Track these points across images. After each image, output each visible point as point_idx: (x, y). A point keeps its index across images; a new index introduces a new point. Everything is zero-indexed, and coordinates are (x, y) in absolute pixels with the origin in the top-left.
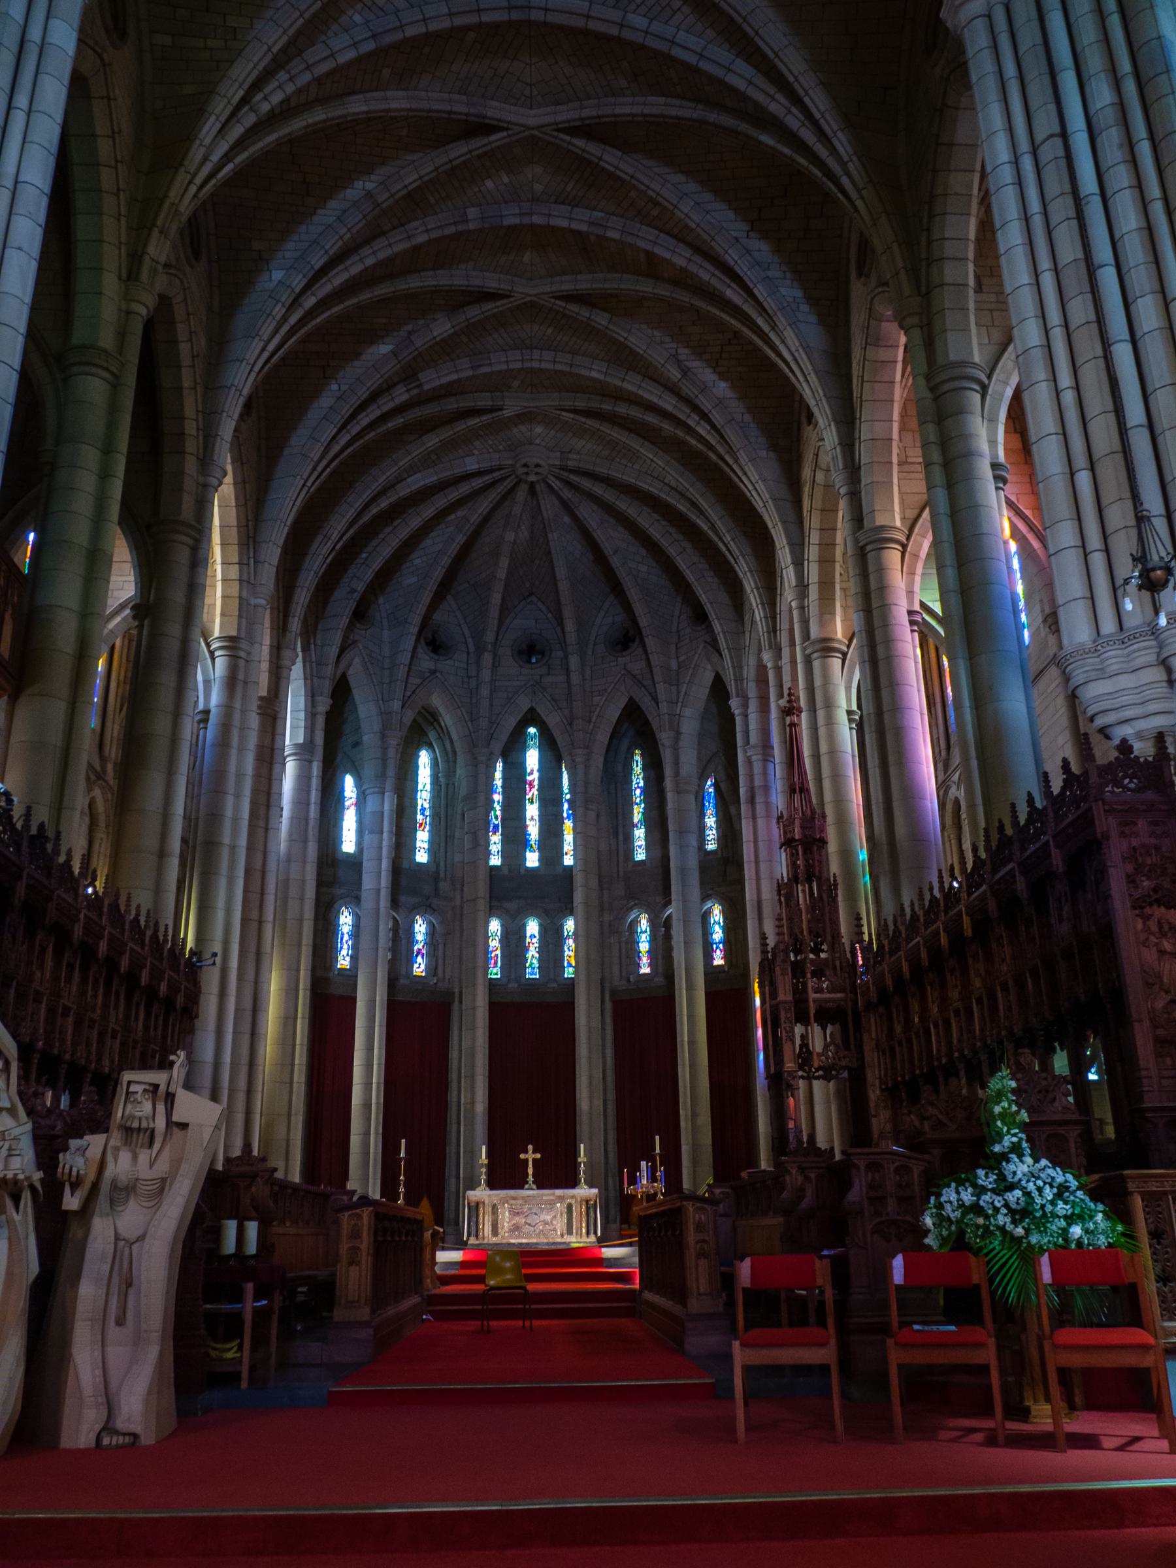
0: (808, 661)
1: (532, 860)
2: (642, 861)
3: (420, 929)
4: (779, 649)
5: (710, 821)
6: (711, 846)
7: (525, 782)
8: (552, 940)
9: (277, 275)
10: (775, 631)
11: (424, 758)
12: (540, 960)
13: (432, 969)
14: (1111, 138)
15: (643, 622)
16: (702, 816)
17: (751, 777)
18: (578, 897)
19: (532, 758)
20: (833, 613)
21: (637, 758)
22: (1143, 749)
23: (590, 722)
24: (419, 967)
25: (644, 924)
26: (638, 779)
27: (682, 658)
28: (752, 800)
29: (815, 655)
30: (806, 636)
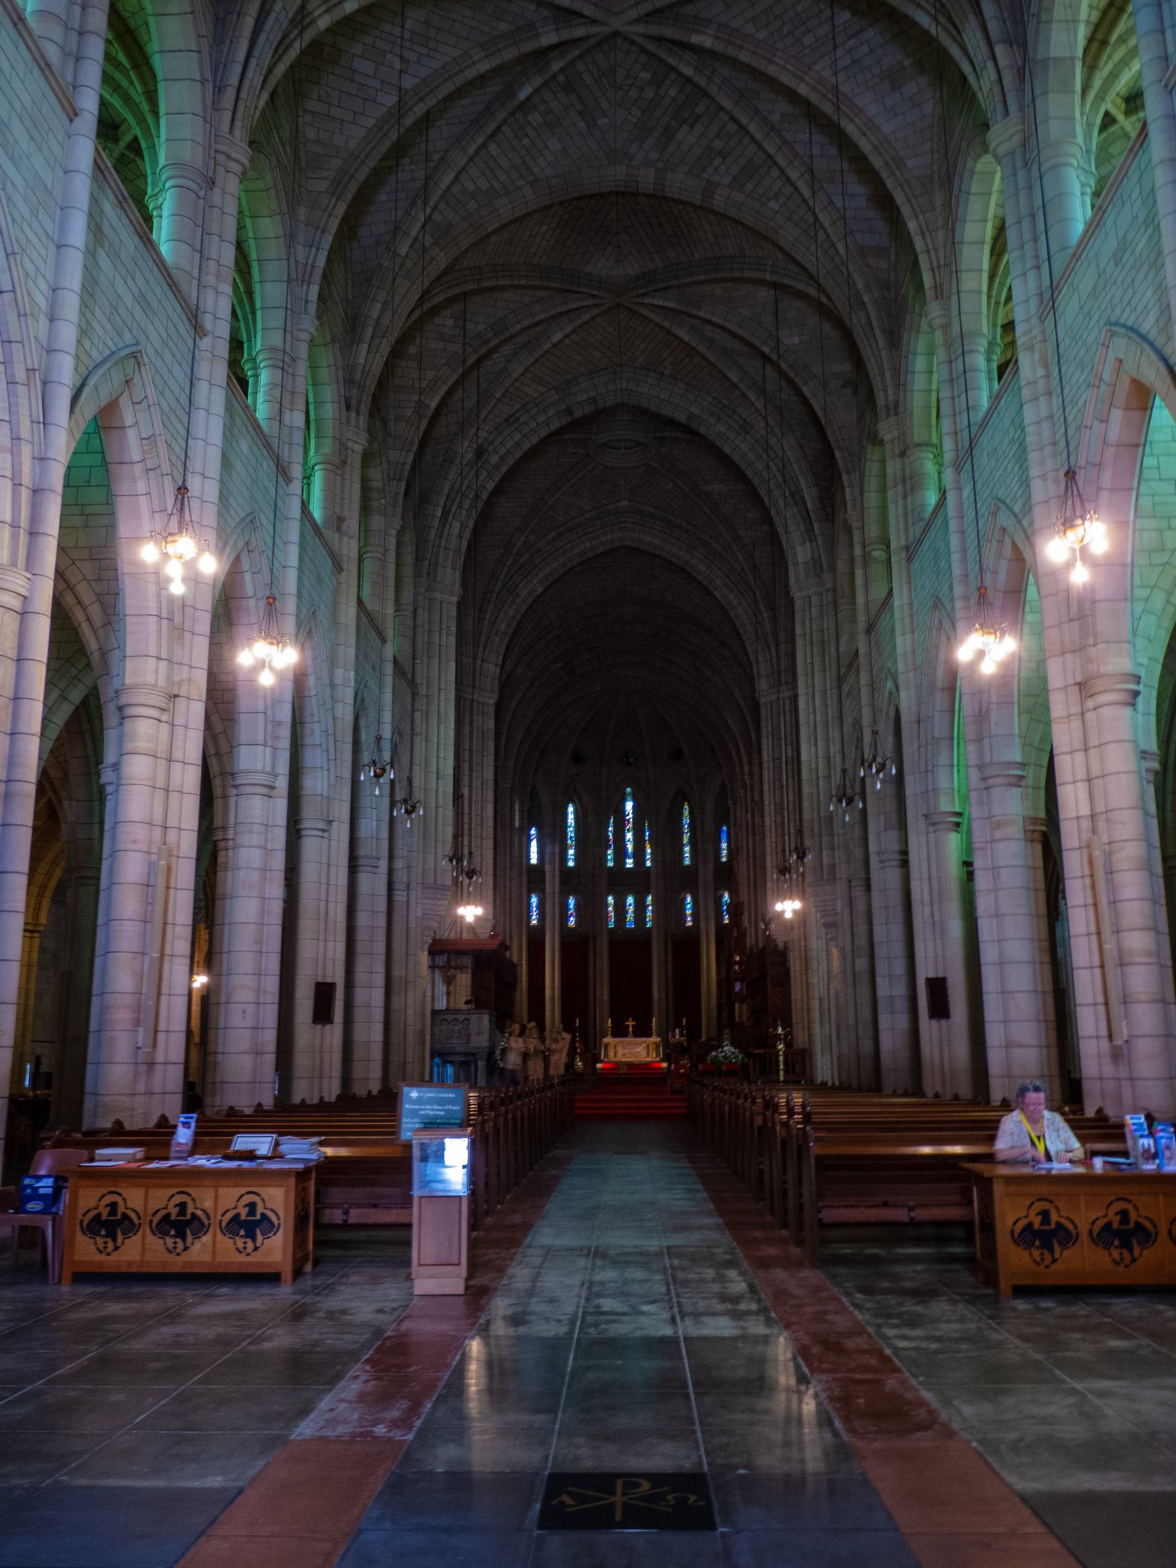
1: (630, 863)
3: (572, 902)
5: (724, 845)
6: (724, 859)
8: (640, 907)
9: (521, 670)
11: (571, 809)
14: (790, 766)
16: (720, 842)
18: (653, 884)
19: (629, 806)
21: (686, 807)
22: (781, 946)
24: (572, 922)
25: (689, 899)
26: (686, 821)
30: (753, 800)
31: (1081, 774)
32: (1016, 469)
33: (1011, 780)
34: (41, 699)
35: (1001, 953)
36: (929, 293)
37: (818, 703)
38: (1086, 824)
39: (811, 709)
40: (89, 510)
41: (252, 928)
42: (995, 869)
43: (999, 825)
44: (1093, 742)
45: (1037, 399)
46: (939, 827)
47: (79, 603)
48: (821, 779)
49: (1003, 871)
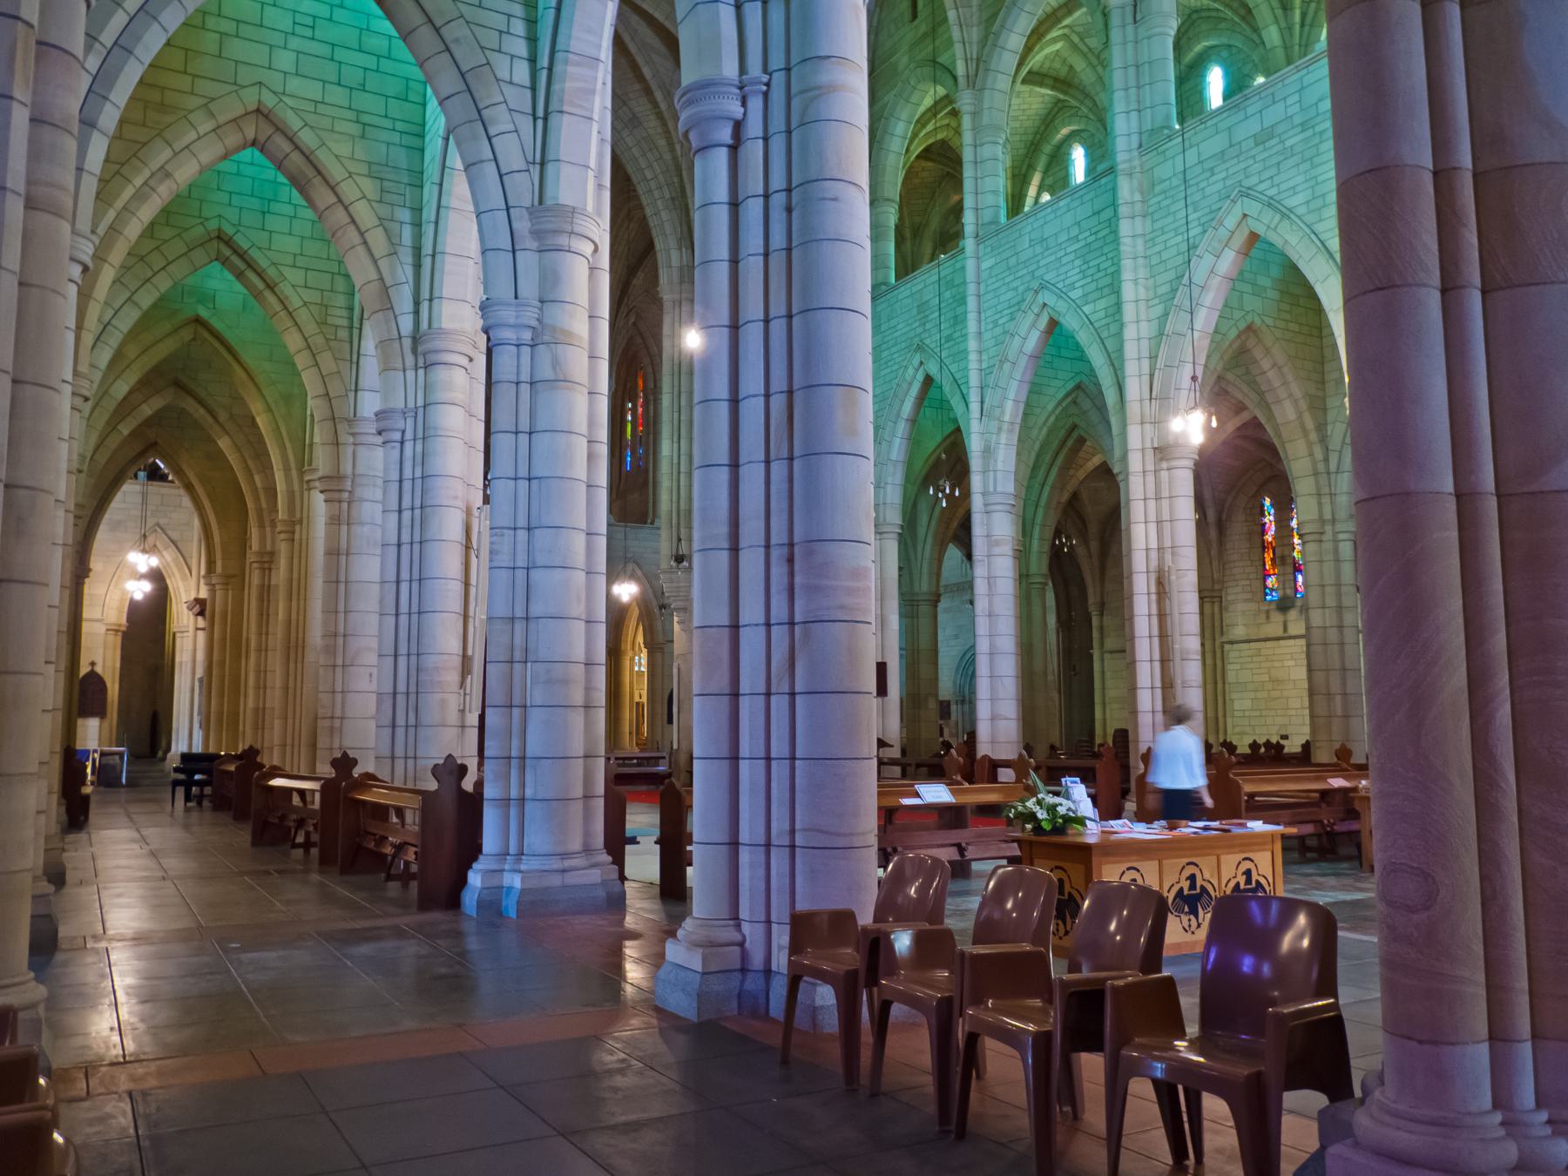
31: (1152, 517)
32: (1078, 262)
33: (1009, 508)
34: (607, 357)
35: (992, 645)
36: (962, 81)
37: (683, 403)
38: (1154, 555)
39: (676, 409)
40: (366, 119)
41: (376, 588)
42: (990, 579)
43: (997, 543)
44: (1165, 493)
45: (1133, 218)
46: (885, 536)
47: (353, 221)
48: (682, 476)
49: (998, 580)
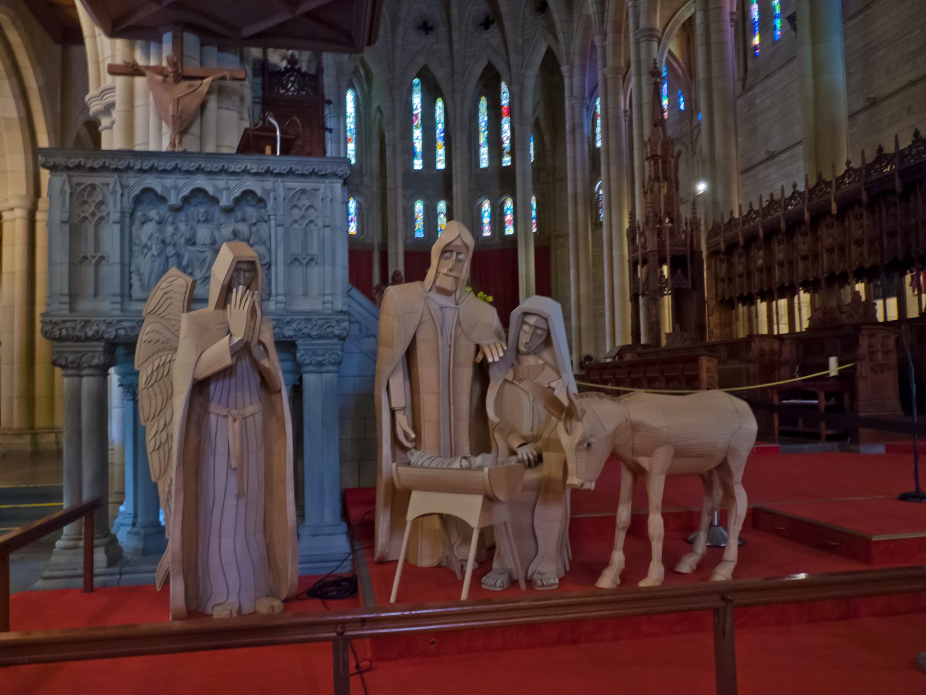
0: (637, 43)
1: (418, 164)
2: (485, 169)
3: (352, 205)
4: (605, 34)
7: (413, 115)
10: (603, 22)
12: (424, 226)
13: (360, 229)
15: (504, 10)
17: (573, 117)
20: (655, 12)
23: (464, 76)
27: (525, 37)
28: (573, 132)
29: (642, 39)
